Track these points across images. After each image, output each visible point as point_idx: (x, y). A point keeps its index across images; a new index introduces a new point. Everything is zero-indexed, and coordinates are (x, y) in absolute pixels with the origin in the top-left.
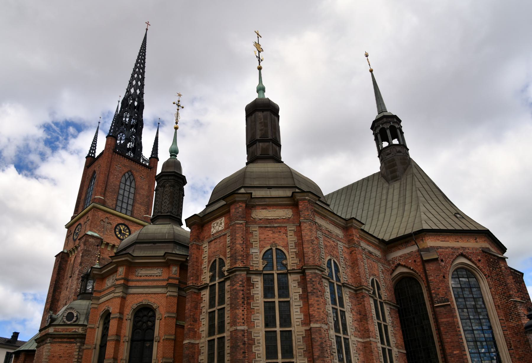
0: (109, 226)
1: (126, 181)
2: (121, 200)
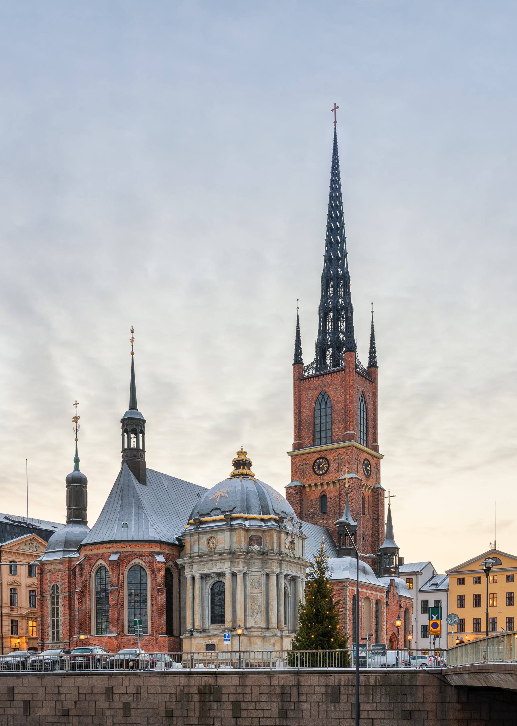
0: (308, 466)
1: (320, 405)
2: (319, 430)
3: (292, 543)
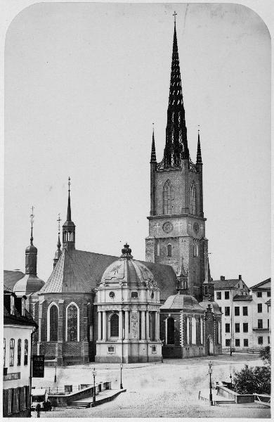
3: (153, 294)
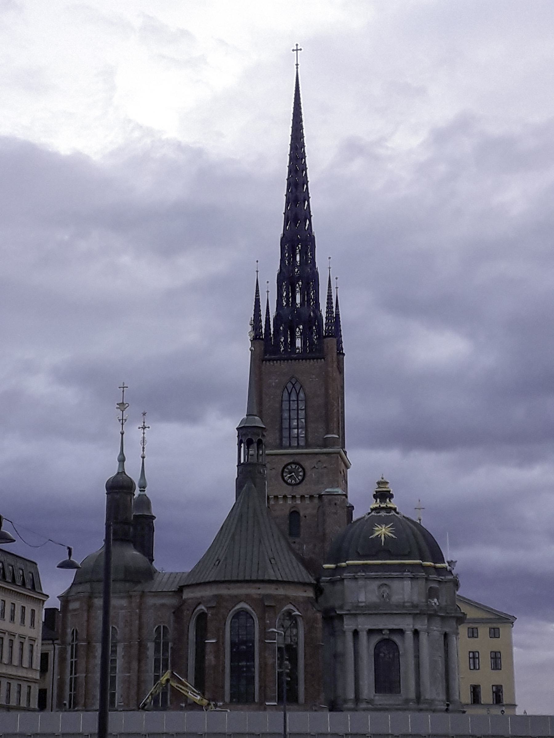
0: (273, 471)
1: (290, 394)
2: (287, 426)
